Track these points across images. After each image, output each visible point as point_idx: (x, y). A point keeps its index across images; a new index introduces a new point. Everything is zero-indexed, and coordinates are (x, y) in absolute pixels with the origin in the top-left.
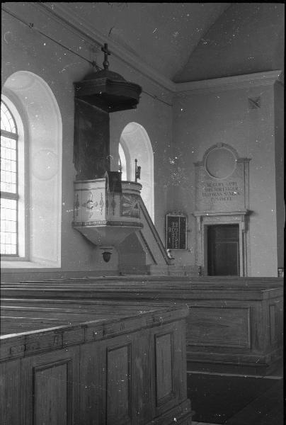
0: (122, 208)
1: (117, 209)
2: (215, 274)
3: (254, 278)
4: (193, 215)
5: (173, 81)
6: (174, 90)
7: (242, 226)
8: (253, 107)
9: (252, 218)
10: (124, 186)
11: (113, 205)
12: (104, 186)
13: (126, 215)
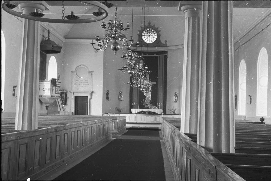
0: (56, 91)
1: (54, 91)
2: (77, 114)
3: (93, 116)
4: (70, 92)
5: (64, 37)
6: (65, 41)
7: (89, 97)
8: (96, 52)
9: (93, 94)
10: (57, 83)
11: (53, 90)
12: (50, 83)
13: (57, 93)
